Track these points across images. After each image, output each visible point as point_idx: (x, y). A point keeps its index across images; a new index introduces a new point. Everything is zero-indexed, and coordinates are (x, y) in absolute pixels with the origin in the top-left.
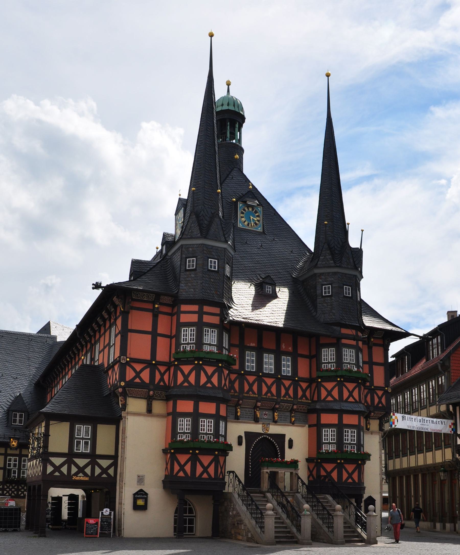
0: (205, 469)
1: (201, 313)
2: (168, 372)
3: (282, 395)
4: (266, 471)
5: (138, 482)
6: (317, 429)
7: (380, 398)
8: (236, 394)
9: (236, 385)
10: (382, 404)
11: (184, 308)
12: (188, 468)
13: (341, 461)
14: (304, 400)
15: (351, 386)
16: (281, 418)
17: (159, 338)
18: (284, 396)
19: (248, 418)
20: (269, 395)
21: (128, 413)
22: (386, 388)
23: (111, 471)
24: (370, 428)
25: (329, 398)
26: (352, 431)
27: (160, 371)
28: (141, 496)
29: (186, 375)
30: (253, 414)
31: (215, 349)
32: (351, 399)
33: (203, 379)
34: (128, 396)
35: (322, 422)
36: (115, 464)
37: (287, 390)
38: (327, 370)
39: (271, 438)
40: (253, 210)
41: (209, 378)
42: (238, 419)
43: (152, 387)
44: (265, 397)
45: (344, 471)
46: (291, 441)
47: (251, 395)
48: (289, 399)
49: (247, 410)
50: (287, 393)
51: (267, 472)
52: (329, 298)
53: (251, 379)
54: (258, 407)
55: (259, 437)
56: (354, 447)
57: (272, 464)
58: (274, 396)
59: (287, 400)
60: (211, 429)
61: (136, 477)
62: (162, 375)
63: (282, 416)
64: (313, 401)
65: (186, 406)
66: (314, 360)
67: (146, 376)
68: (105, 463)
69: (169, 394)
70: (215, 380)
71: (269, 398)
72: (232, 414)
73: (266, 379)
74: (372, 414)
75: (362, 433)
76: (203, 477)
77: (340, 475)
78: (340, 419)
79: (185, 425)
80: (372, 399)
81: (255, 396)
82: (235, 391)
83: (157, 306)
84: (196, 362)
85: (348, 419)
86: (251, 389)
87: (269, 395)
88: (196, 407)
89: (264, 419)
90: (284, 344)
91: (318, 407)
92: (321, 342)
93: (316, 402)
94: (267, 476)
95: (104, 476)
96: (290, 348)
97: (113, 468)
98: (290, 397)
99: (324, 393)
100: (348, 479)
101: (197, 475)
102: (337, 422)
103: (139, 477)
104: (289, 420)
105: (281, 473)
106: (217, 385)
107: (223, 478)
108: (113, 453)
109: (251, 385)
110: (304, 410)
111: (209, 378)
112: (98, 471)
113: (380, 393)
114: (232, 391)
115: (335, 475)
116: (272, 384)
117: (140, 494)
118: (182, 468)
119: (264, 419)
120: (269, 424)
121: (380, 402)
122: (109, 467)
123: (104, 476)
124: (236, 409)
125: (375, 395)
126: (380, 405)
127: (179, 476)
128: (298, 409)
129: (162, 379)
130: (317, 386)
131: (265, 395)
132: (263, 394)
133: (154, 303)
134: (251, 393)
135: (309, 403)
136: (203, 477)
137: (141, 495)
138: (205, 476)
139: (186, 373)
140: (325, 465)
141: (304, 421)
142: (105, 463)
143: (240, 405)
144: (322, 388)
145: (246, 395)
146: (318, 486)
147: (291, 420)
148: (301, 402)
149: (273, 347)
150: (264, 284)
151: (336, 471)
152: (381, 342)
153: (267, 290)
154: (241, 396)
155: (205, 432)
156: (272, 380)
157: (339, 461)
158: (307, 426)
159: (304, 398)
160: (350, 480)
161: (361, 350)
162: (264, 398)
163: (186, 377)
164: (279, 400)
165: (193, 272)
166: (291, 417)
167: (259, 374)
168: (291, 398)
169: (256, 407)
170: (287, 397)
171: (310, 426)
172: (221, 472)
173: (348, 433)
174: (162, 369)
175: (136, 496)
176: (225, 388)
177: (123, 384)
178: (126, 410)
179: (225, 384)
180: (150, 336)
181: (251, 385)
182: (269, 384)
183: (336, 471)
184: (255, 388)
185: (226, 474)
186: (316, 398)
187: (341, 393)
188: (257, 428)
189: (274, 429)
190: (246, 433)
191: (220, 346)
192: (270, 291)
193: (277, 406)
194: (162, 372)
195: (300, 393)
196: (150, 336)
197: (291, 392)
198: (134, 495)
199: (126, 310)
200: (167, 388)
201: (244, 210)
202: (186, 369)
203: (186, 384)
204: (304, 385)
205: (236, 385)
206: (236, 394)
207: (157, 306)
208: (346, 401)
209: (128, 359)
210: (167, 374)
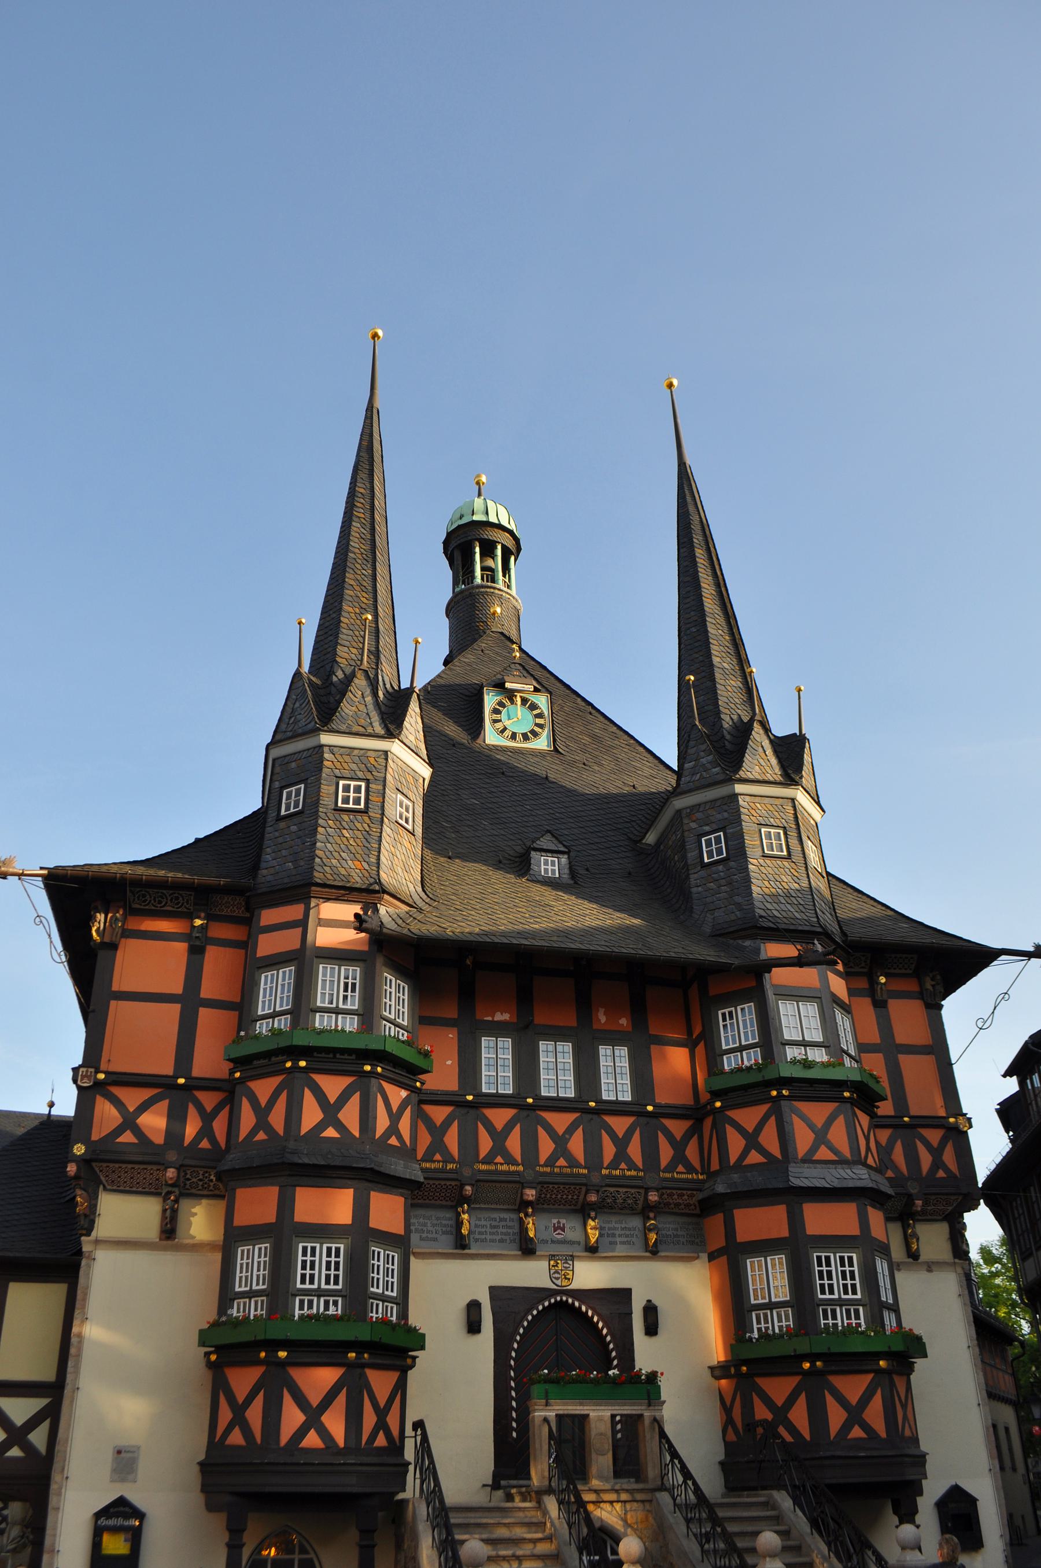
0: (314, 1418)
2: (227, 1109)
3: (607, 1161)
4: (545, 1413)
5: (114, 1471)
6: (731, 1260)
8: (450, 1166)
9: (452, 1139)
10: (947, 1170)
11: (269, 916)
12: (255, 1414)
13: (813, 1364)
14: (680, 1173)
15: (818, 1112)
16: (614, 1235)
17: (203, 1012)
18: (614, 1165)
19: (501, 1241)
20: (562, 1162)
21: (97, 1242)
22: (952, 1120)
23: (38, 1438)
24: (922, 1253)
25: (754, 1157)
26: (842, 1258)
28: (120, 1522)
29: (265, 1109)
30: (517, 1230)
31: (350, 1024)
32: (823, 1153)
33: (311, 1115)
34: (105, 1189)
35: (741, 1237)
36: (52, 1414)
37: (621, 1144)
38: (739, 1070)
39: (582, 1302)
40: (524, 701)
41: (331, 1111)
42: (464, 1247)
43: (172, 1156)
44: (548, 1169)
45: (830, 1399)
46: (651, 1311)
47: (500, 1168)
48: (628, 1173)
49: (496, 1215)
50: (621, 1155)
51: (546, 1420)
52: (721, 868)
53: (500, 1117)
54: (529, 1203)
55: (541, 1301)
56: (857, 1312)
57: (560, 1384)
58: (578, 1166)
59: (624, 1177)
60: (336, 1277)
61: (109, 1455)
62: (208, 1119)
63: (615, 1229)
64: (711, 1175)
65: (258, 1204)
66: (700, 1049)
69: (212, 1172)
70: (350, 1115)
71: (561, 1174)
72: (444, 1233)
73: (551, 1117)
74: (919, 1203)
75: (881, 1267)
76: (305, 1443)
77: (817, 1415)
78: (795, 1221)
79: (253, 1265)
81: (513, 1168)
82: (448, 1158)
83: (198, 922)
84: (289, 1064)
85: (820, 1219)
86: (499, 1147)
87: (562, 1162)
88: (286, 1205)
89: (553, 1242)
90: (602, 1011)
91: (721, 1188)
92: (713, 991)
93: (716, 1173)
94: (545, 1430)
96: (623, 1021)
97: (44, 1427)
98: (632, 1166)
99: (735, 1144)
100: (846, 1427)
101: (285, 1437)
102: (785, 1233)
103: (119, 1452)
104: (638, 1241)
105: (600, 1419)
107: (396, 1447)
108: (48, 1375)
109: (499, 1137)
110: (688, 1205)
111: (331, 1111)
113: (934, 1136)
114: (438, 1157)
115: (799, 1415)
116: (571, 1130)
117: (117, 1515)
118: (239, 1411)
119: (553, 1242)
120: (572, 1258)
122: (32, 1423)
124: (458, 1215)
125: (919, 1144)
127: (230, 1446)
128: (668, 1204)
130: (714, 1125)
131: (545, 1165)
132: (542, 1162)
133: (191, 917)
134: (499, 1159)
135: (698, 1181)
136: (305, 1443)
137: (119, 1516)
138: (312, 1440)
139: (263, 1101)
140: (763, 1382)
141: (692, 1243)
143: (467, 1200)
144: (729, 1129)
145: (483, 1167)
146: (753, 1456)
147: (646, 1239)
148: (673, 1179)
149: (569, 1019)
150: (533, 853)
151: (802, 1401)
152: (912, 986)
153: (546, 870)
154: (467, 1172)
155: (315, 1286)
156: (571, 1117)
157: (807, 1365)
158: (704, 1256)
159: (680, 1168)
160: (857, 1432)
161: (846, 1009)
162: (545, 1174)
163: (262, 1113)
164: (595, 1180)
165: (295, 820)
166: (646, 1230)
167: (527, 1103)
168: (639, 1170)
169: (524, 1204)
170: (623, 1166)
171: (712, 1257)
172: (381, 1425)
173: (828, 1264)
174: (209, 1100)
175: (103, 1522)
176: (393, 1141)
177: (79, 1149)
178: (94, 1233)
179: (393, 1129)
180: (176, 1008)
181: (499, 1137)
182: (560, 1131)
183: (802, 1401)
184: (514, 1143)
185: (409, 1431)
186: (715, 1166)
187: (785, 1137)
188: (531, 1274)
189: (589, 1275)
190: (496, 1292)
191: (369, 1012)
192: (553, 871)
193: (593, 1198)
194: (209, 1109)
195: (666, 1153)
196: (174, 1010)
197: (635, 1150)
198: (98, 1515)
199: (107, 940)
200: (217, 1154)
201: (503, 705)
202: (263, 1088)
203: (261, 1136)
204: (678, 1127)
205: (452, 1139)
206: (450, 1166)
207: (198, 922)
208: (808, 1160)
209: (101, 1076)
210: (224, 1114)
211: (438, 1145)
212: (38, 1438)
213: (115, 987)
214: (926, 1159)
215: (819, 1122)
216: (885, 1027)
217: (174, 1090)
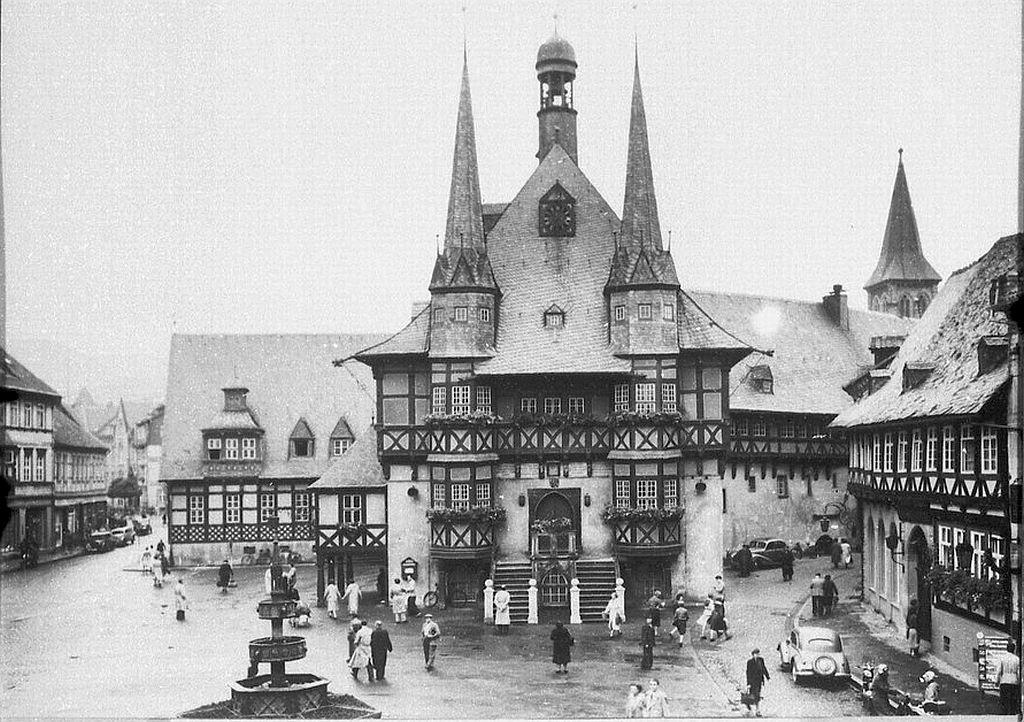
1: (449, 373)
7: (713, 435)
9: (511, 440)
11: (435, 367)
12: (444, 538)
23: (383, 540)
27: (420, 436)
36: (386, 533)
46: (587, 498)
62: (423, 439)
67: (405, 443)
68: (376, 532)
78: (633, 471)
80: (701, 437)
85: (641, 471)
95: (376, 545)
106: (469, 448)
112: (369, 540)
121: (713, 438)
122: (380, 536)
123: (376, 545)
126: (713, 443)
129: (423, 443)
142: (376, 532)
202: (438, 434)
205: (511, 440)
211: (506, 442)
212: (383, 540)
213: (385, 394)
214: (707, 436)
215: (646, 434)
216: (699, 383)
217: (411, 430)
